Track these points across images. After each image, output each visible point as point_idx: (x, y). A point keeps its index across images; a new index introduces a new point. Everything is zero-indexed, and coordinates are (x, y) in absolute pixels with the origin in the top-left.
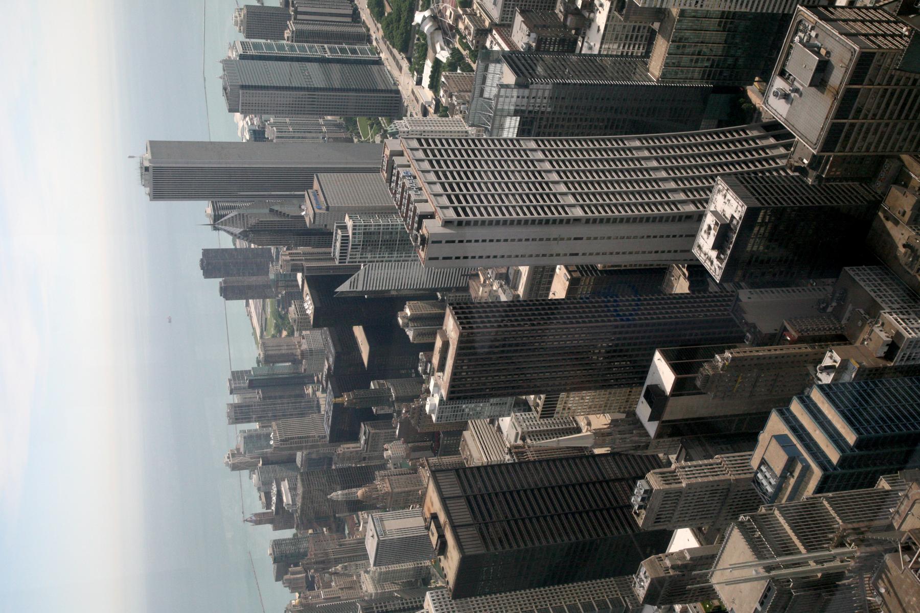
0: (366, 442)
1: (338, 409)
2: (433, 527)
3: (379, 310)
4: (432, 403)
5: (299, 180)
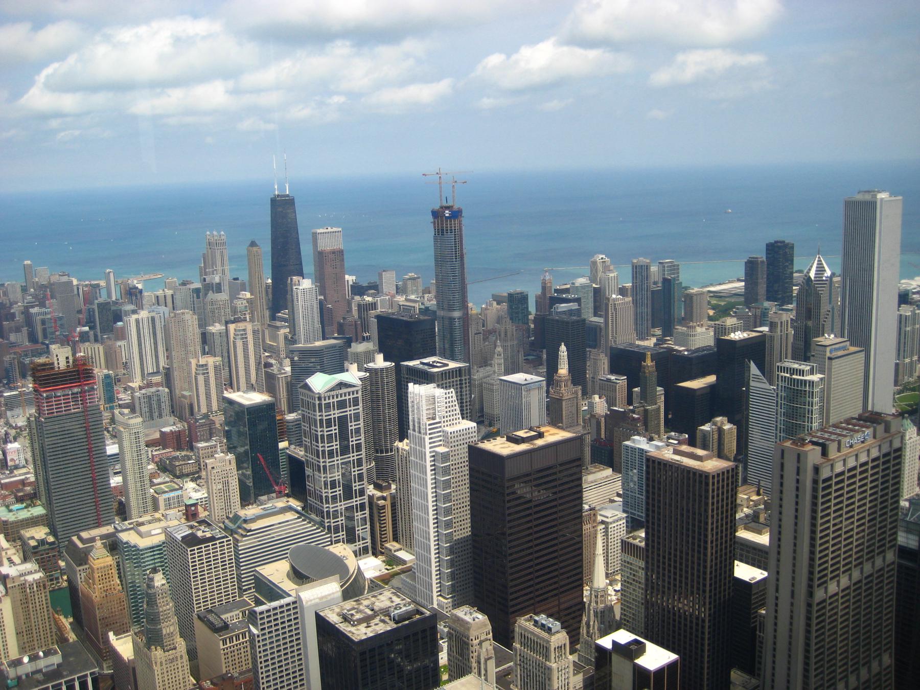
0: (609, 380)
1: (640, 356)
2: (533, 433)
3: (729, 400)
4: (640, 442)
5: (859, 335)
